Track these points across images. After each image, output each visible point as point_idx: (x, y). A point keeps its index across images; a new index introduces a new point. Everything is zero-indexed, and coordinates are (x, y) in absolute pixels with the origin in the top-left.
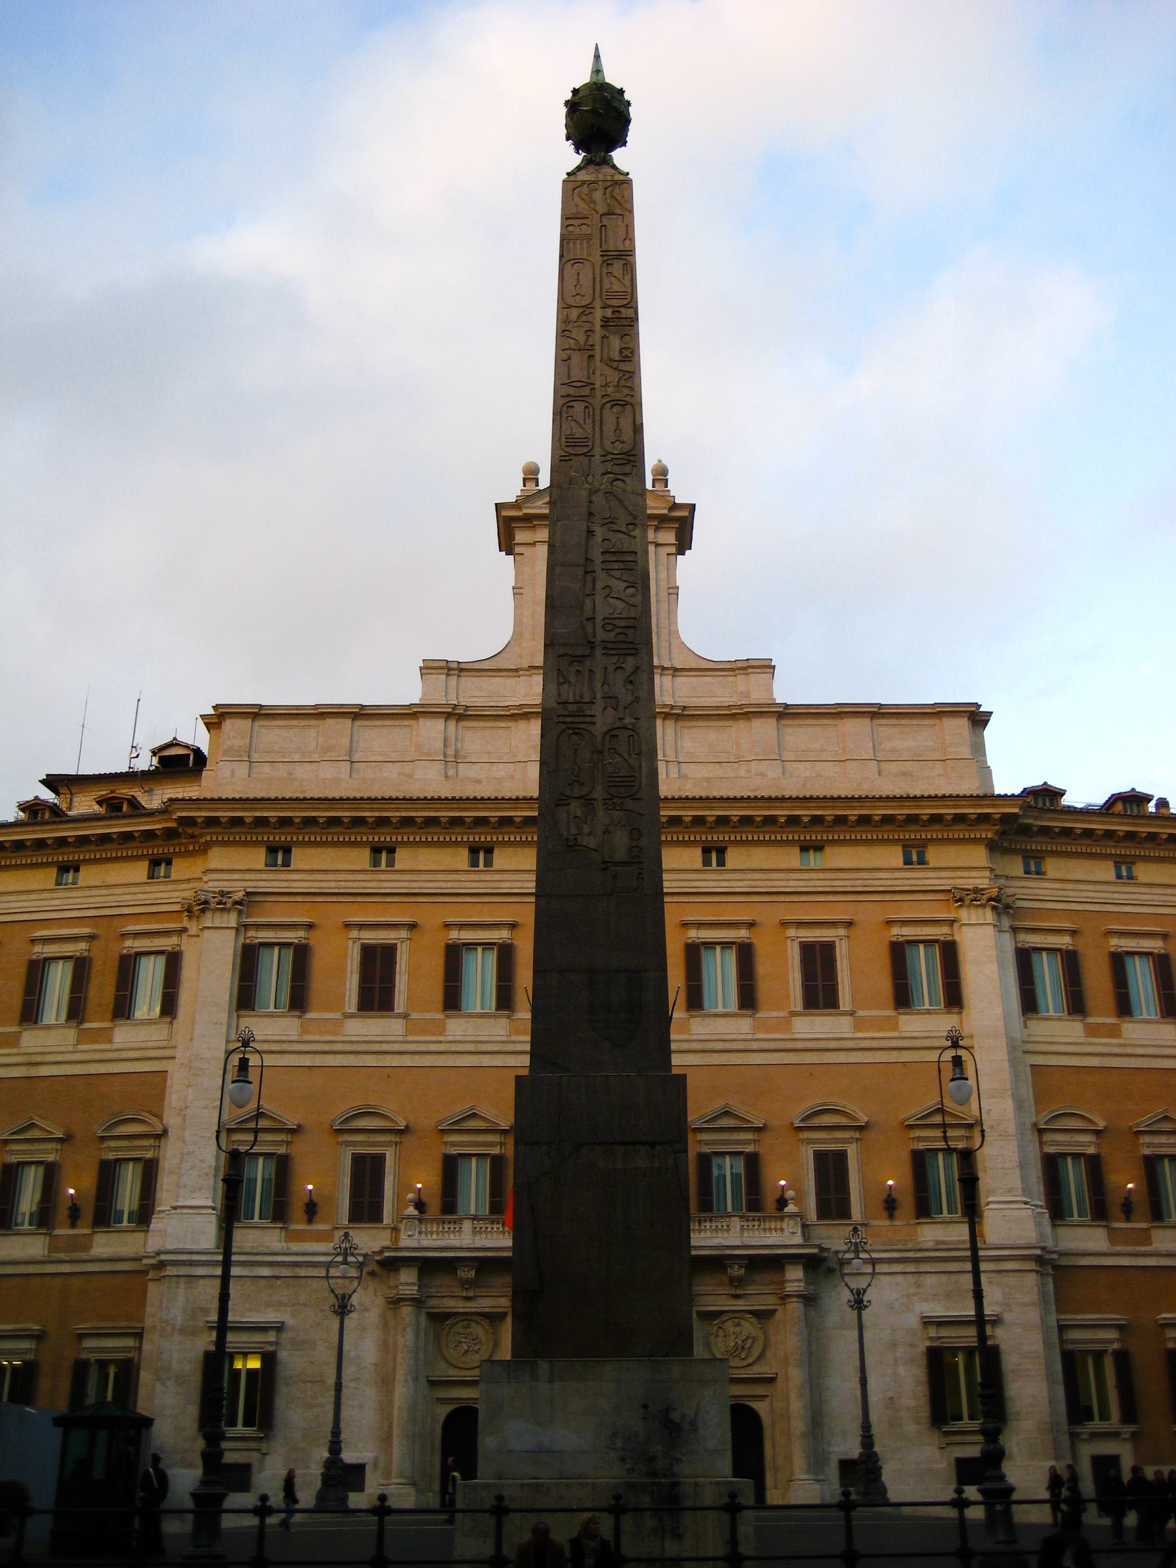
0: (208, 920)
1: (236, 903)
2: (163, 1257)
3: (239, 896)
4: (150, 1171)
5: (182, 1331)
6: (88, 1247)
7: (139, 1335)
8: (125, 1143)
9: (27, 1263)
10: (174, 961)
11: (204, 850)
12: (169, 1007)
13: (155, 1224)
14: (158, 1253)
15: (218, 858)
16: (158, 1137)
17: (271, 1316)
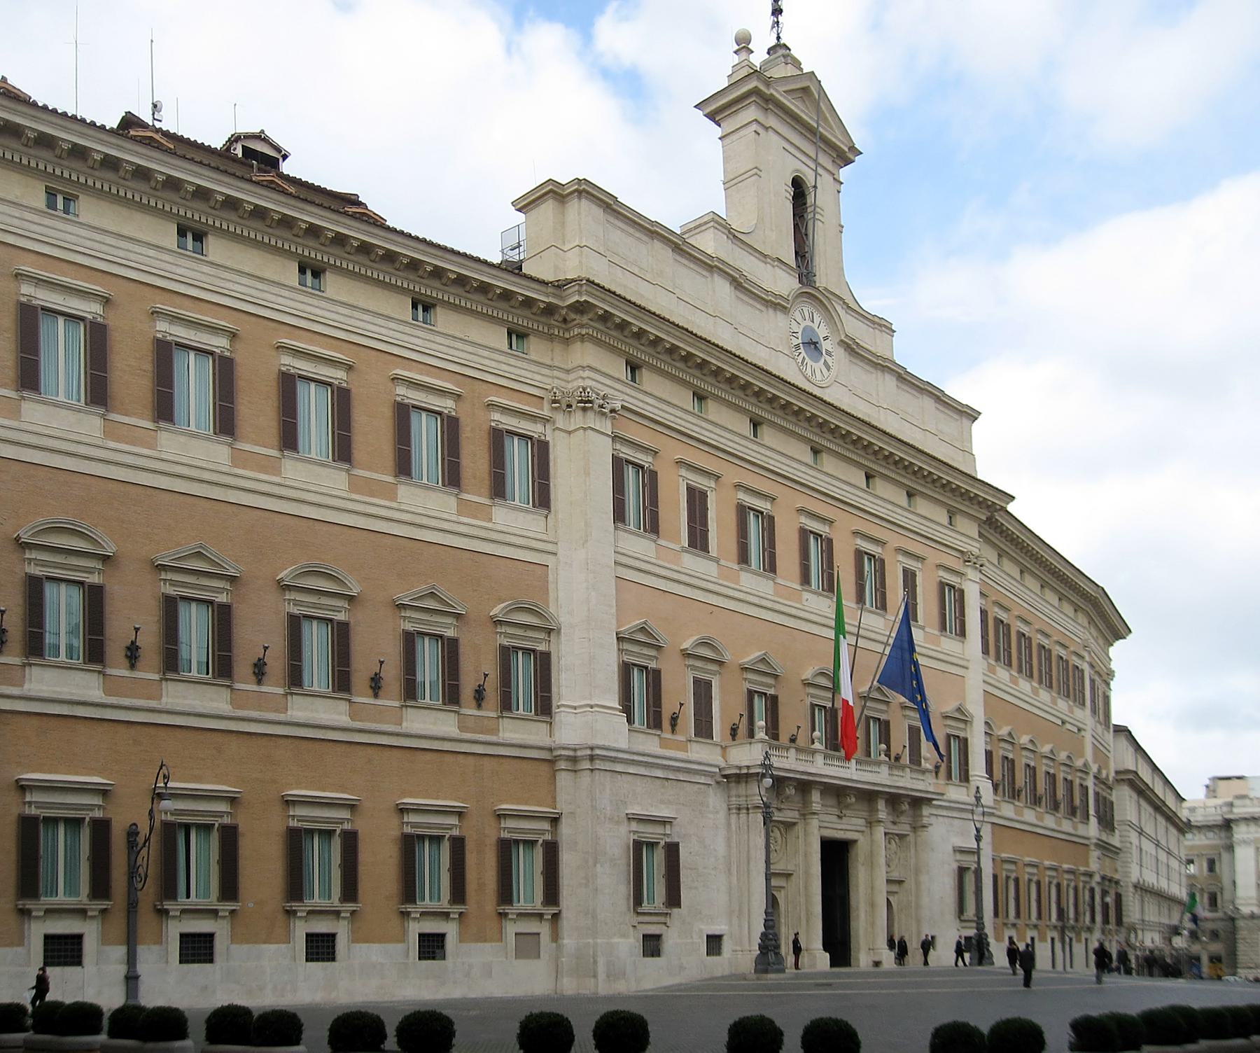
0: (592, 420)
1: (613, 411)
2: (598, 752)
3: (618, 405)
4: (543, 663)
5: (611, 819)
6: (495, 731)
7: (555, 821)
8: (520, 632)
9: (443, 739)
10: (541, 452)
11: (567, 342)
12: (542, 499)
13: (563, 717)
14: (592, 749)
15: (585, 354)
16: (549, 631)
17: (664, 812)
